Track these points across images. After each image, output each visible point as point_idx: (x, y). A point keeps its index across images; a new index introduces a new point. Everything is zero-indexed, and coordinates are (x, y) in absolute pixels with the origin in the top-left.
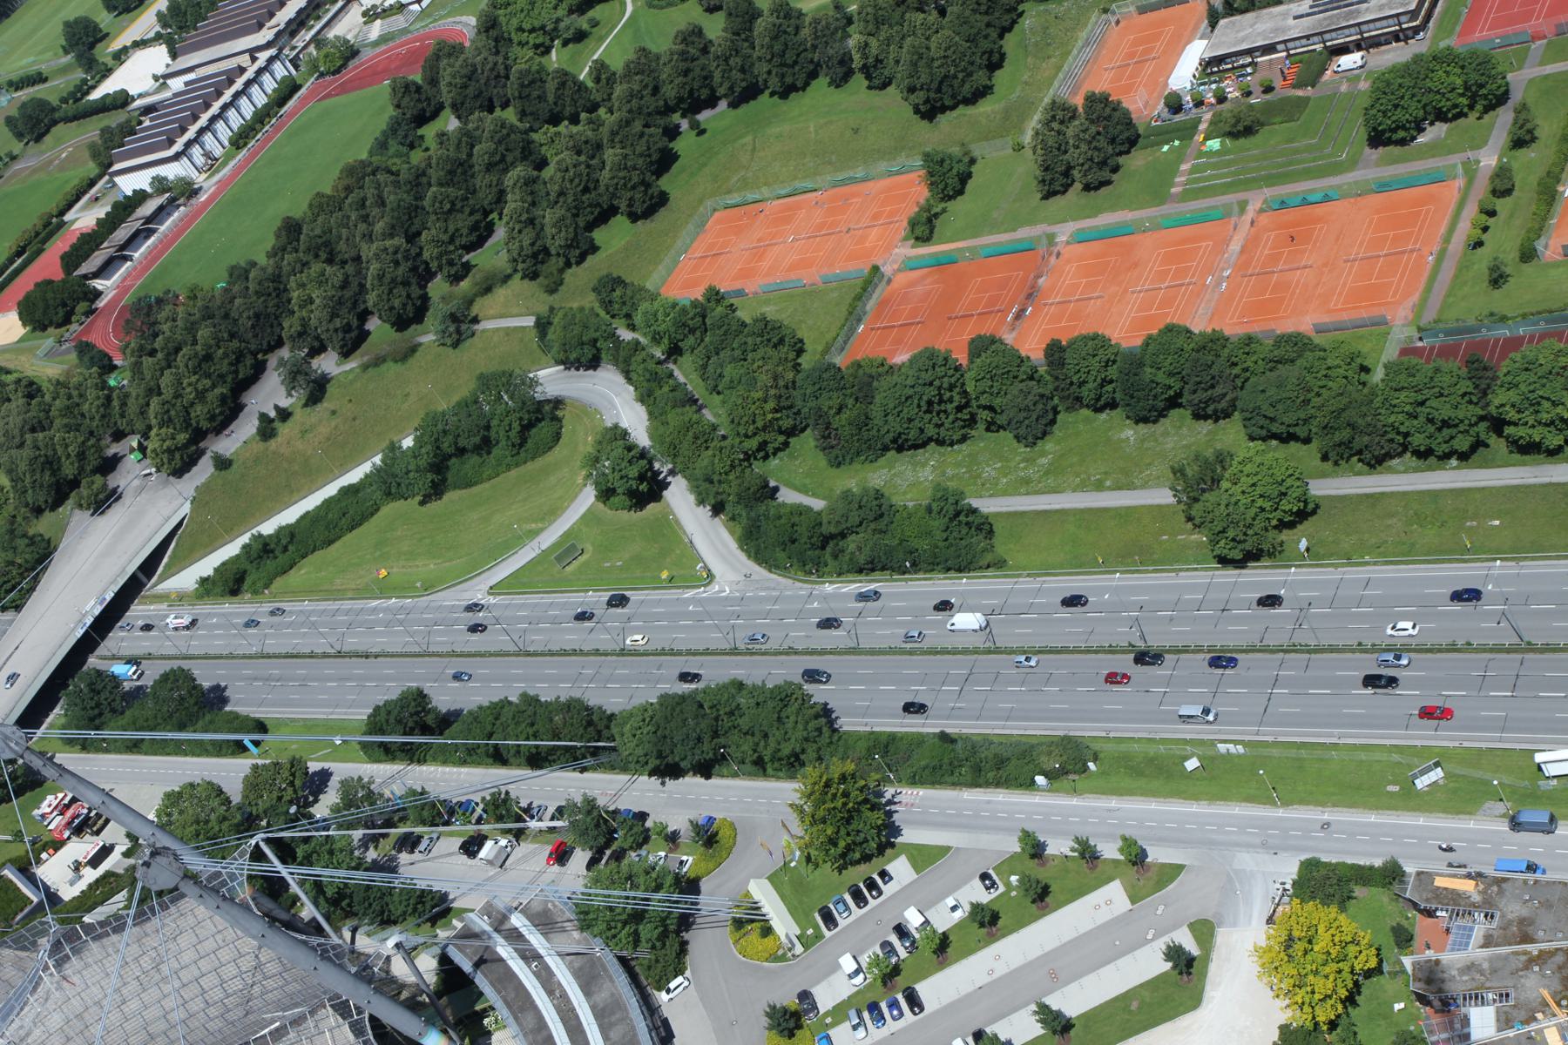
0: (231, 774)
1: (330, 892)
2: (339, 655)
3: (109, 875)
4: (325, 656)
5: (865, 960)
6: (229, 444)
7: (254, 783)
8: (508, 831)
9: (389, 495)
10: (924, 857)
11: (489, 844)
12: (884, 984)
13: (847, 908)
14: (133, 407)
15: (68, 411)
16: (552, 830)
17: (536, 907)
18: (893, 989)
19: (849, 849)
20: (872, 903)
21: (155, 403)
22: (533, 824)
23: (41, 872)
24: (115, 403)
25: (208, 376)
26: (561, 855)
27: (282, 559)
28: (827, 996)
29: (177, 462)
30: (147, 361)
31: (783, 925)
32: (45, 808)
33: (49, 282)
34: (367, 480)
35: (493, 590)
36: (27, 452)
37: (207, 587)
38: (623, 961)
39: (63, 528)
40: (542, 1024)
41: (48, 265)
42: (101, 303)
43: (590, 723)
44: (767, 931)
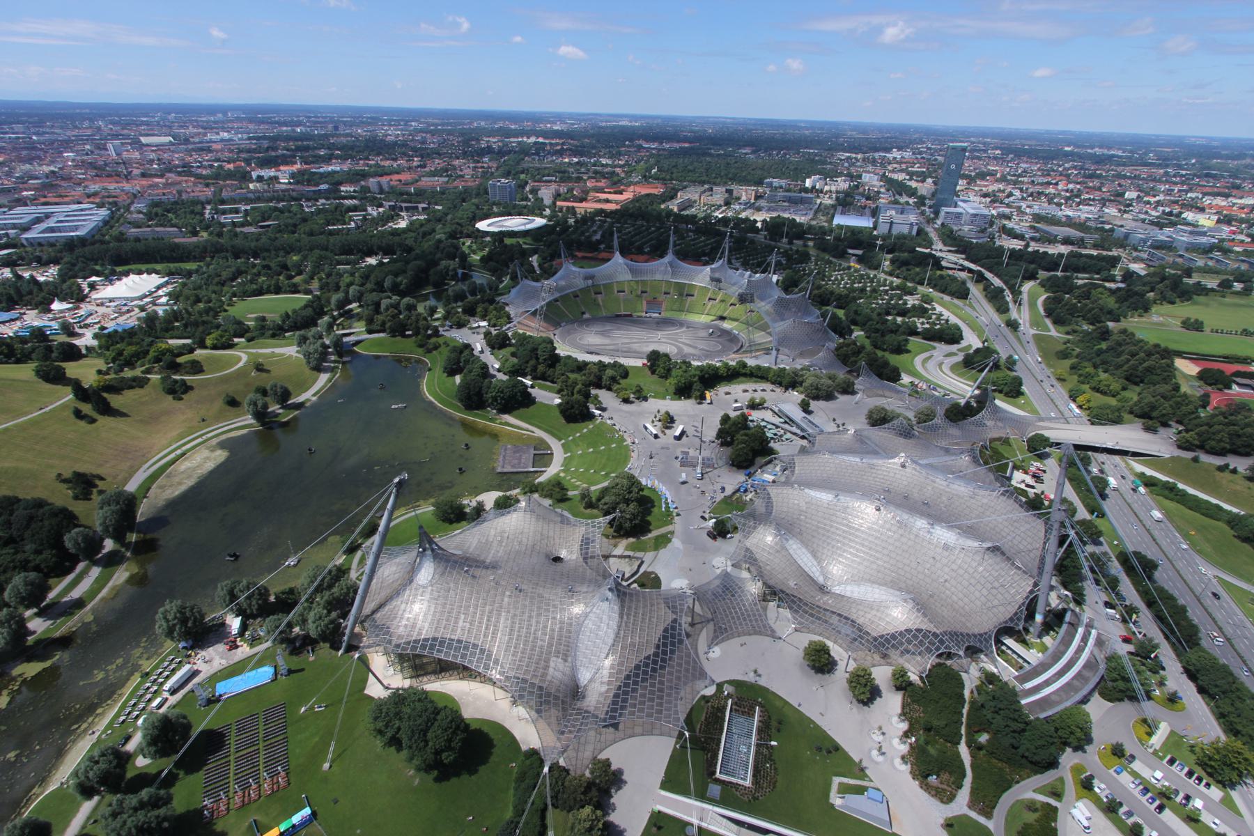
0: (1082, 513)
1: (1065, 563)
2: (1148, 531)
3: (1026, 491)
4: (1144, 526)
5: (1166, 784)
6: (1205, 458)
7: (1083, 523)
8: (1122, 615)
9: (1229, 523)
10: (1228, 802)
11: (1113, 611)
12: (1160, 793)
13: (1182, 769)
14: (1196, 422)
15: (1177, 403)
16: (1134, 633)
17: (1103, 638)
18: (1160, 799)
19: (1212, 767)
20: (1191, 781)
21: (1205, 428)
22: (1131, 625)
23: (1015, 472)
24: (1193, 416)
25: (1230, 439)
26: (1126, 640)
27: (1171, 495)
28: (1137, 766)
29: (1184, 445)
30: (1221, 418)
31: (1157, 740)
32: (1035, 464)
33: (1222, 372)
34: (1230, 512)
35: (1215, 577)
36: (1153, 400)
37: (1142, 476)
38: (1103, 676)
39: (1130, 422)
40: (1063, 653)
41: (1230, 368)
42: (1226, 391)
43: (1191, 636)
44: (1150, 734)
